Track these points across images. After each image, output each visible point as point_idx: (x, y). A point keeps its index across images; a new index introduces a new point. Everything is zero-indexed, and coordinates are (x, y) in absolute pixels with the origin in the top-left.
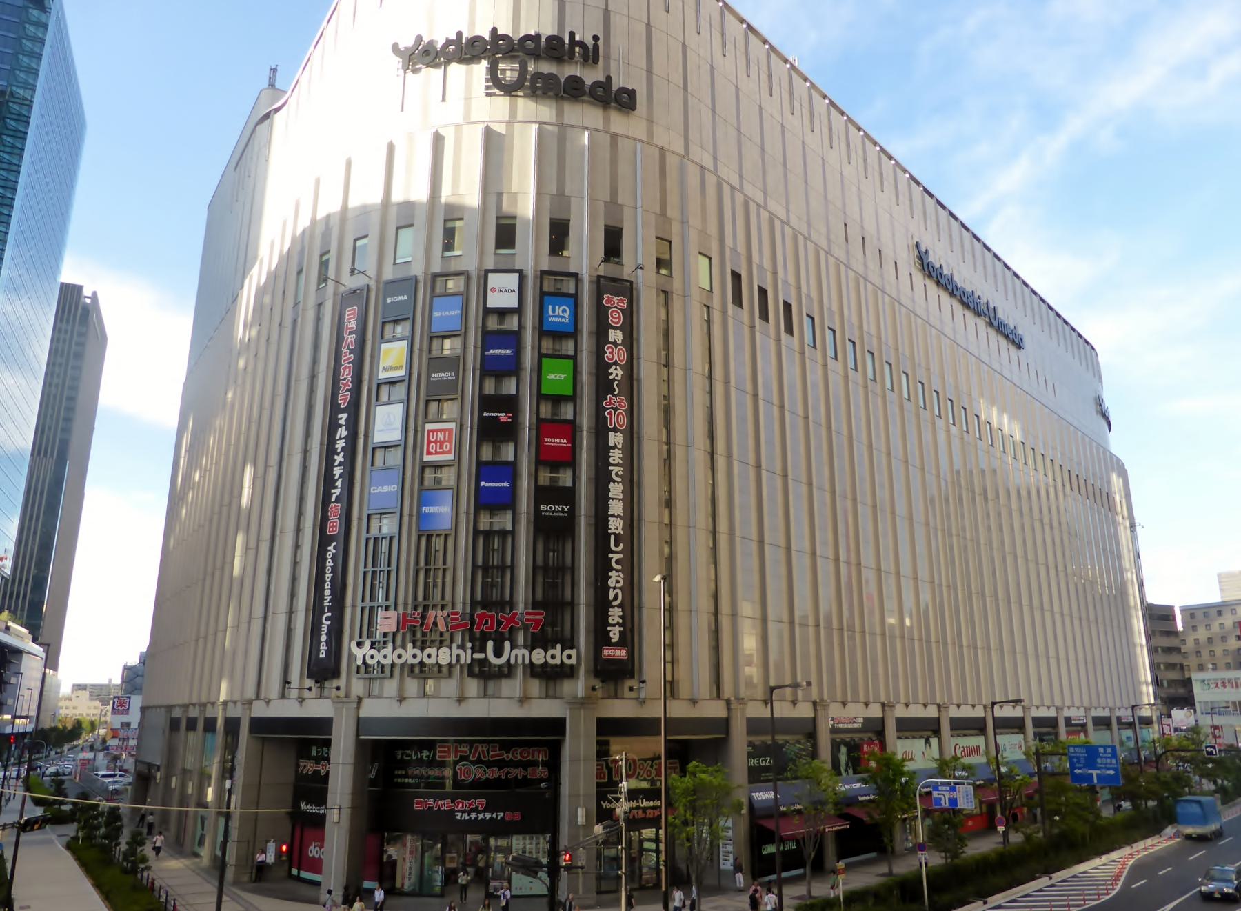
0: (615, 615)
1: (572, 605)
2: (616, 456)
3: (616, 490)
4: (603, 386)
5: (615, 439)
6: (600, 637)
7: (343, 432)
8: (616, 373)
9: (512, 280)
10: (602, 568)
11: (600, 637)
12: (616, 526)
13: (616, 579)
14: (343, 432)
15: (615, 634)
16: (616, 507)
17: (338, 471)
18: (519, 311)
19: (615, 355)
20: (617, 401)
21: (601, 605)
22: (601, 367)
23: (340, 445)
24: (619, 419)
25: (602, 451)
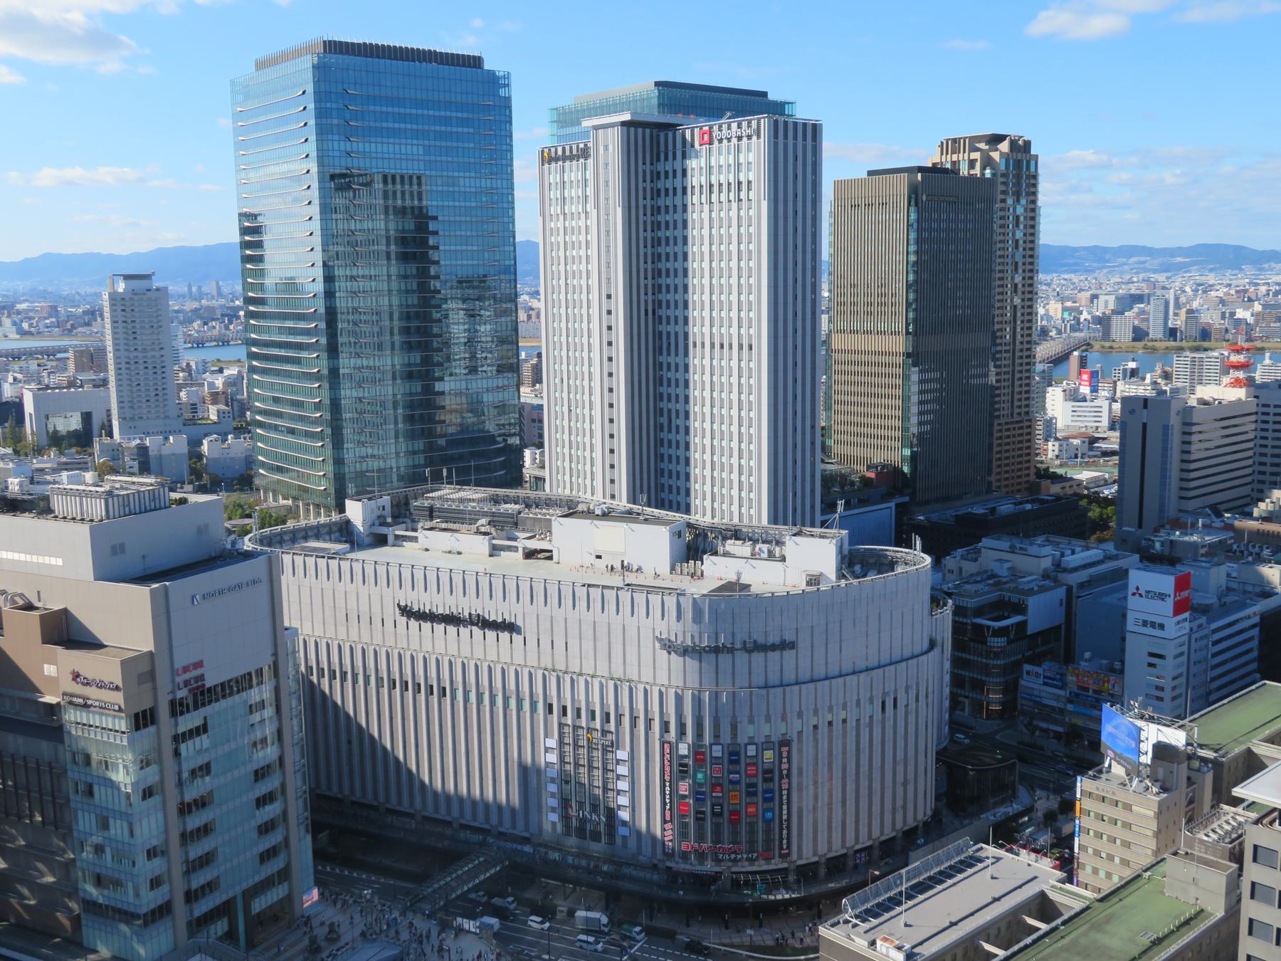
0: (785, 842)
1: (774, 840)
2: (785, 797)
3: (785, 807)
4: (781, 777)
5: (785, 792)
6: (781, 848)
7: (668, 788)
8: (785, 772)
9: (754, 747)
10: (781, 829)
11: (781, 848)
12: (785, 817)
13: (785, 832)
14: (668, 788)
15: (785, 847)
16: (785, 812)
17: (668, 801)
18: (756, 756)
19: (785, 766)
20: (785, 781)
21: (781, 839)
22: (781, 771)
23: (668, 792)
24: (785, 786)
25: (781, 796)
